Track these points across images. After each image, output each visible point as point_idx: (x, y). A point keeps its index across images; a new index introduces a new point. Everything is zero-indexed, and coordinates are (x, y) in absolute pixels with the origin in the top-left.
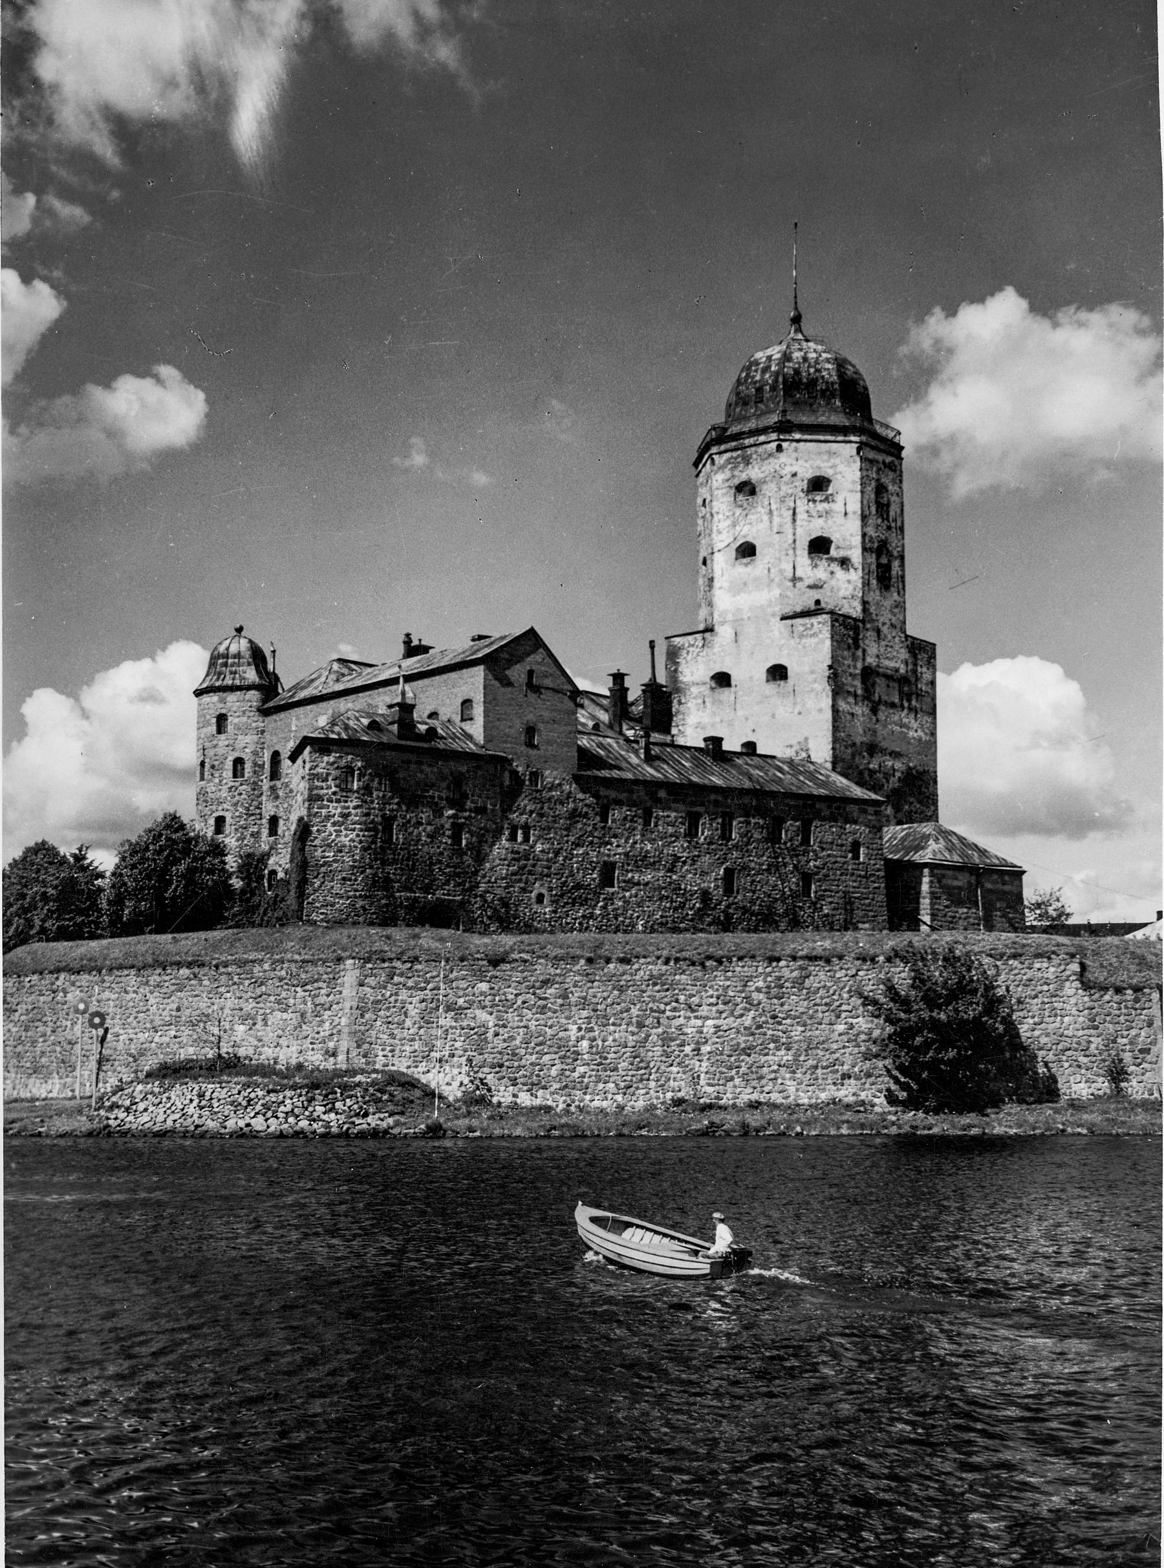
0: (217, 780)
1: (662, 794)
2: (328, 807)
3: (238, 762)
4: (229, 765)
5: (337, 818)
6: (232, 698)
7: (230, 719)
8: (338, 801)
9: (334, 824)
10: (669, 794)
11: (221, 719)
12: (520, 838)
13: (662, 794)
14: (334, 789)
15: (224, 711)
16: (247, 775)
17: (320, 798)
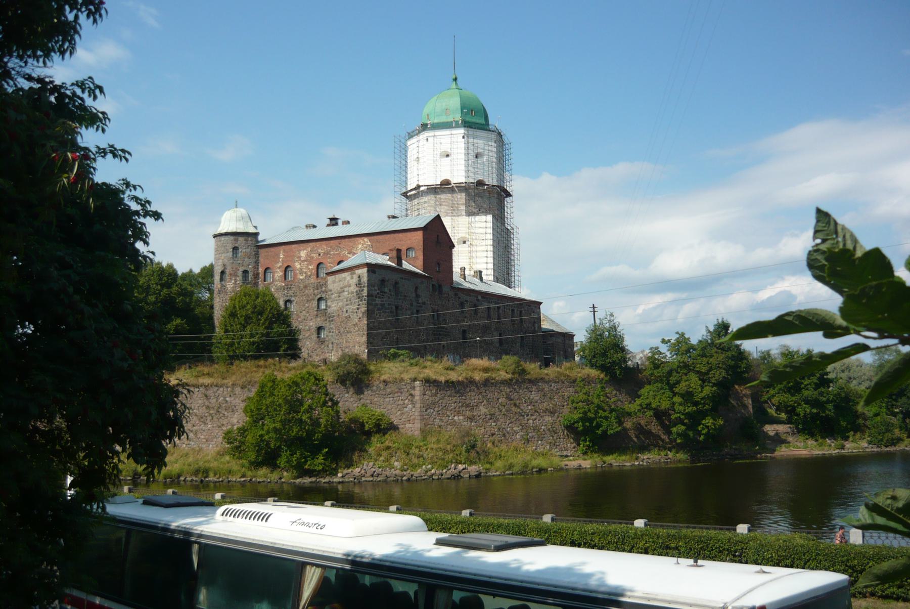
0: (233, 281)
1: (480, 298)
2: (375, 301)
3: (245, 272)
4: (240, 273)
5: (379, 306)
6: (241, 239)
7: (240, 250)
8: (379, 298)
9: (378, 309)
10: (483, 297)
11: (235, 249)
12: (436, 318)
13: (480, 298)
14: (378, 291)
15: (236, 245)
16: (250, 279)
17: (372, 296)
